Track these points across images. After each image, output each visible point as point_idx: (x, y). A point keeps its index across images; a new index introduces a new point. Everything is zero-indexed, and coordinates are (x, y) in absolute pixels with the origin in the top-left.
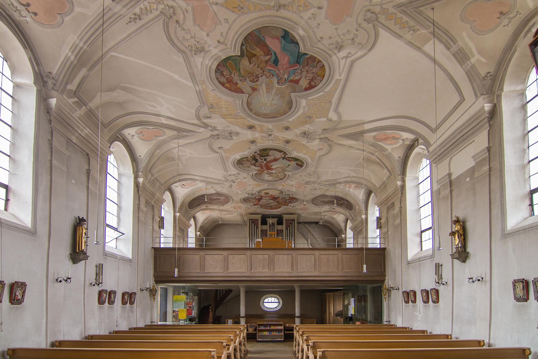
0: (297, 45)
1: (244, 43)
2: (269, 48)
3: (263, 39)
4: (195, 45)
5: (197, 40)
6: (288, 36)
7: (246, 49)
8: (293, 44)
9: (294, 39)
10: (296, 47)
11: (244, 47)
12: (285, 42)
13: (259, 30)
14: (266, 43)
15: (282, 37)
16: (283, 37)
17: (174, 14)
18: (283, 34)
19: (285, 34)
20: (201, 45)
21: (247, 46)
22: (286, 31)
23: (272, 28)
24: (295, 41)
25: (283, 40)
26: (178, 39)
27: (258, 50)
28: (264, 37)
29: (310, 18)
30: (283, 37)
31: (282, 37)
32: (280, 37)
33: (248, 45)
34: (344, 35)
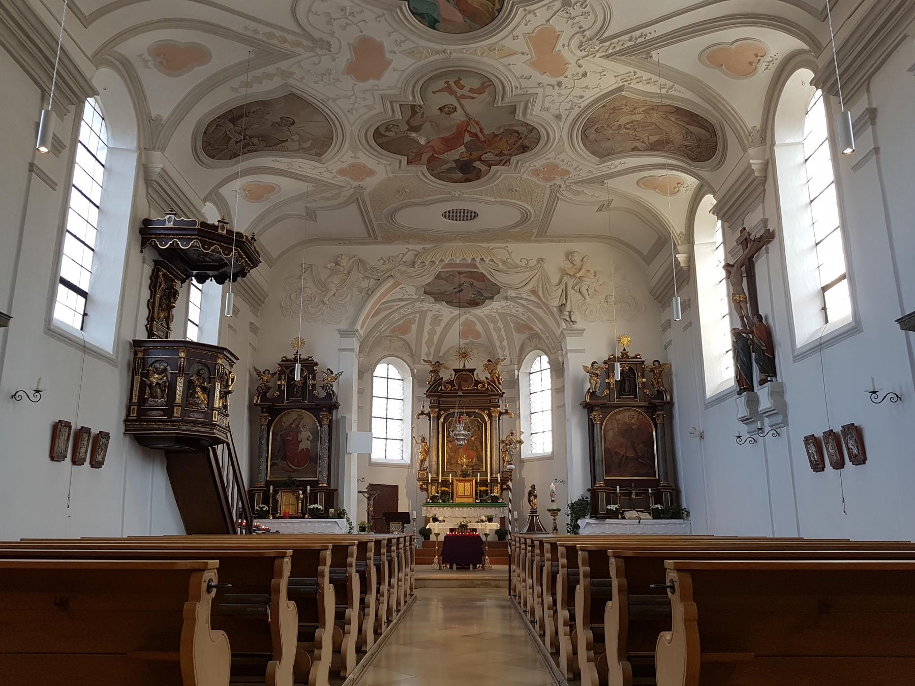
0: (414, 11)
1: (497, 13)
2: (457, 7)
3: (467, 20)
4: (574, 9)
5: (567, 16)
6: (429, 22)
7: (494, 5)
8: (421, 12)
9: (420, 19)
10: (414, 8)
11: (498, 6)
12: (433, 15)
13: (471, 30)
14: (461, 13)
15: (438, 22)
16: (436, 21)
17: (582, 43)
18: (437, 24)
19: (434, 27)
20: (564, 9)
21: (493, 9)
22: (434, 28)
23: (454, 32)
24: (416, 16)
25: (436, 17)
26: (596, 16)
27: (475, 5)
28: (465, 22)
29: (403, 42)
30: (436, 21)
31: (438, 22)
32: (441, 22)
33: (491, 10)
34: (347, 24)
